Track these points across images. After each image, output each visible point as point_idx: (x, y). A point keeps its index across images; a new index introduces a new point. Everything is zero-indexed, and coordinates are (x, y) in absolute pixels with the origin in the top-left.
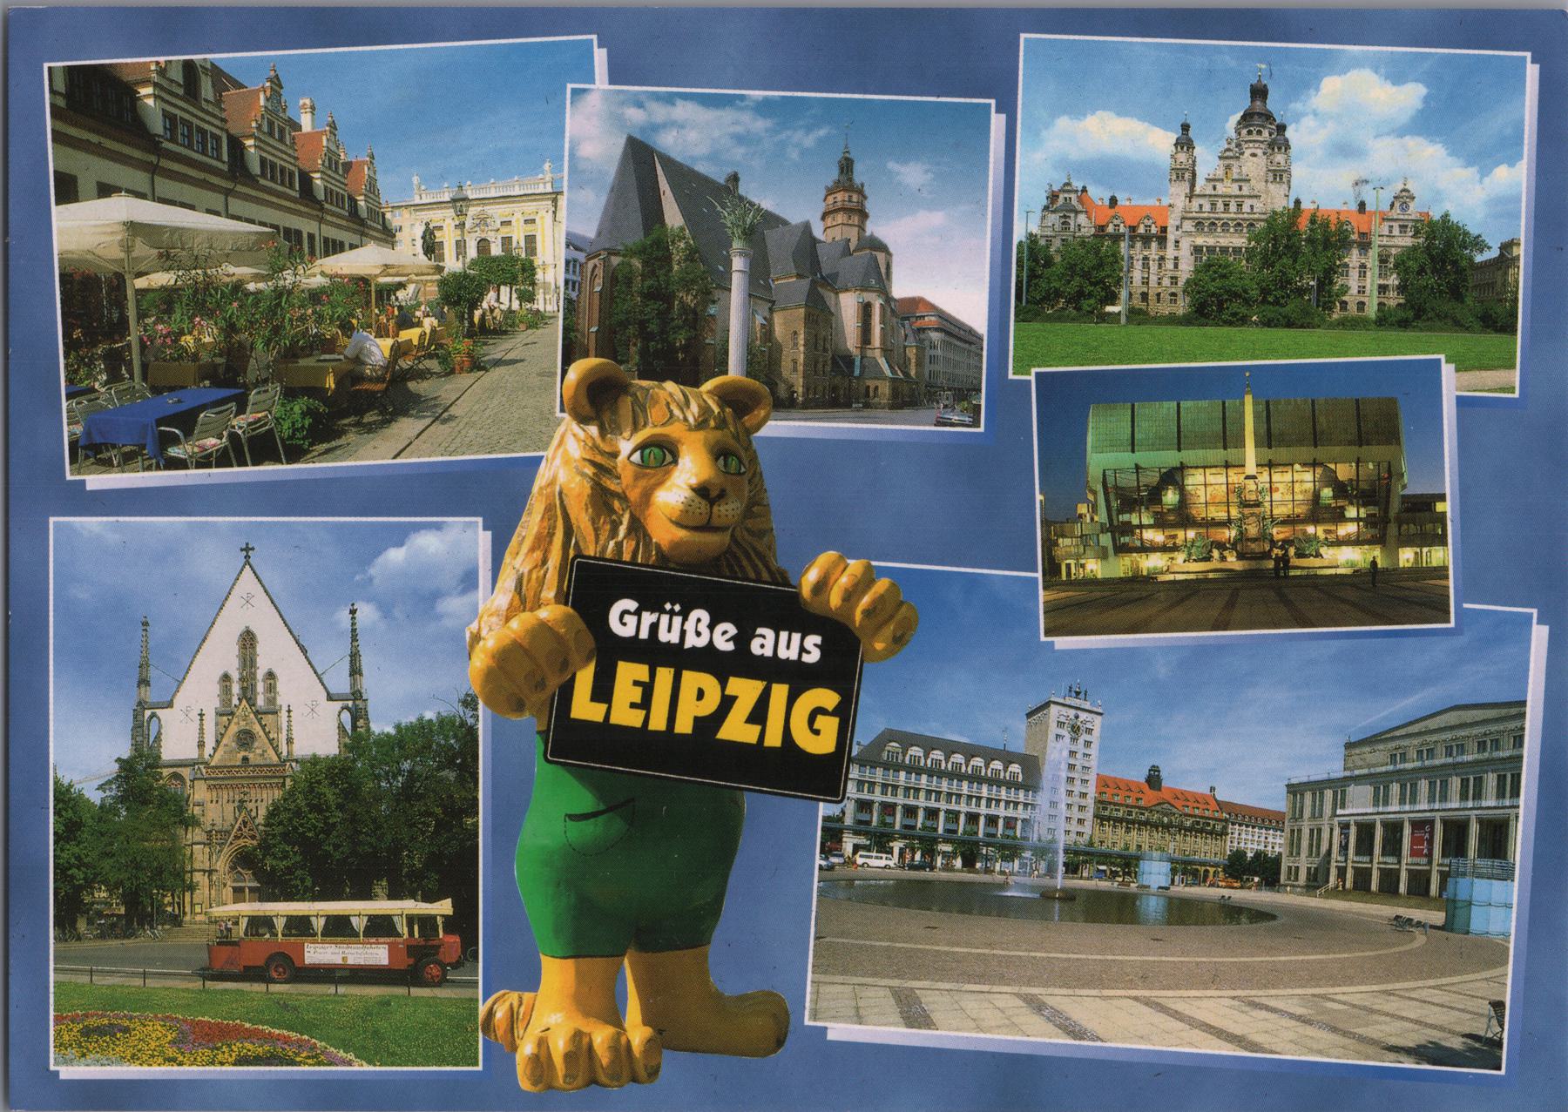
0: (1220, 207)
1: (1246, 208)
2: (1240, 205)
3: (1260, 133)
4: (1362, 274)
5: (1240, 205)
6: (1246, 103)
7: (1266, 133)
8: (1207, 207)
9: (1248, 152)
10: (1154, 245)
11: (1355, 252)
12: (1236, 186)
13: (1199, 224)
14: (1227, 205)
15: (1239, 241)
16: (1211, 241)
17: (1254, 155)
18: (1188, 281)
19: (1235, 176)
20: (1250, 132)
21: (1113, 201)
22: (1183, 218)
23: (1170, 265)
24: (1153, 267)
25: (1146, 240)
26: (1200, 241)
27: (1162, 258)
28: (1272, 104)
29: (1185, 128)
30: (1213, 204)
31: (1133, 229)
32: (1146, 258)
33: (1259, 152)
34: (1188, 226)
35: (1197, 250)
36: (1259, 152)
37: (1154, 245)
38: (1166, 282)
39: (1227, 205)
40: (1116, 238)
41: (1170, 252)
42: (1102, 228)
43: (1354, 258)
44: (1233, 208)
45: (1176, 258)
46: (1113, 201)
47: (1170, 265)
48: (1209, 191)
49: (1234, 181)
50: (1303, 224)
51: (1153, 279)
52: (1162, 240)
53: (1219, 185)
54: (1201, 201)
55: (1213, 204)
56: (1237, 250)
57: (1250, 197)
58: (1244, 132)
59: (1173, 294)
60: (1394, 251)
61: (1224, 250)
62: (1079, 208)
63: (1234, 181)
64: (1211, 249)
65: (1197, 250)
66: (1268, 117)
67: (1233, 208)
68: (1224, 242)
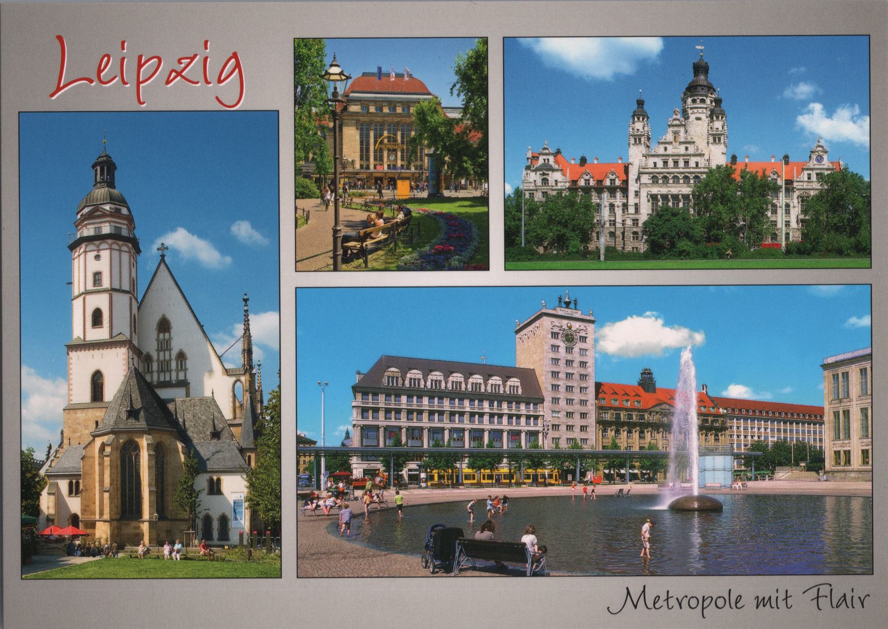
0: (671, 163)
1: (692, 164)
2: (686, 163)
3: (703, 101)
4: (788, 212)
5: (686, 163)
6: (690, 77)
7: (709, 102)
8: (660, 164)
9: (692, 117)
10: (619, 194)
11: (782, 195)
12: (683, 147)
13: (655, 179)
14: (676, 163)
15: (686, 190)
16: (664, 190)
17: (698, 119)
18: (644, 224)
19: (682, 140)
20: (694, 101)
21: (583, 161)
22: (640, 173)
23: (632, 210)
24: (619, 212)
25: (612, 190)
26: (655, 190)
27: (625, 206)
28: (713, 77)
29: (640, 103)
30: (666, 163)
31: (600, 182)
32: (612, 206)
33: (703, 116)
34: (645, 179)
35: (654, 198)
36: (703, 116)
37: (619, 194)
38: (629, 222)
39: (676, 163)
40: (587, 190)
41: (632, 200)
42: (574, 182)
43: (782, 199)
44: (681, 164)
45: (636, 205)
46: (583, 161)
47: (632, 210)
48: (661, 151)
49: (681, 143)
50: (737, 176)
51: (619, 220)
52: (625, 190)
53: (669, 147)
54: (656, 160)
55: (666, 163)
56: (686, 197)
57: (694, 155)
58: (689, 100)
59: (635, 233)
60: (812, 193)
61: (675, 197)
62: (556, 167)
63: (681, 143)
64: (665, 197)
65: (654, 198)
66: (710, 89)
67: (681, 164)
68: (674, 190)
